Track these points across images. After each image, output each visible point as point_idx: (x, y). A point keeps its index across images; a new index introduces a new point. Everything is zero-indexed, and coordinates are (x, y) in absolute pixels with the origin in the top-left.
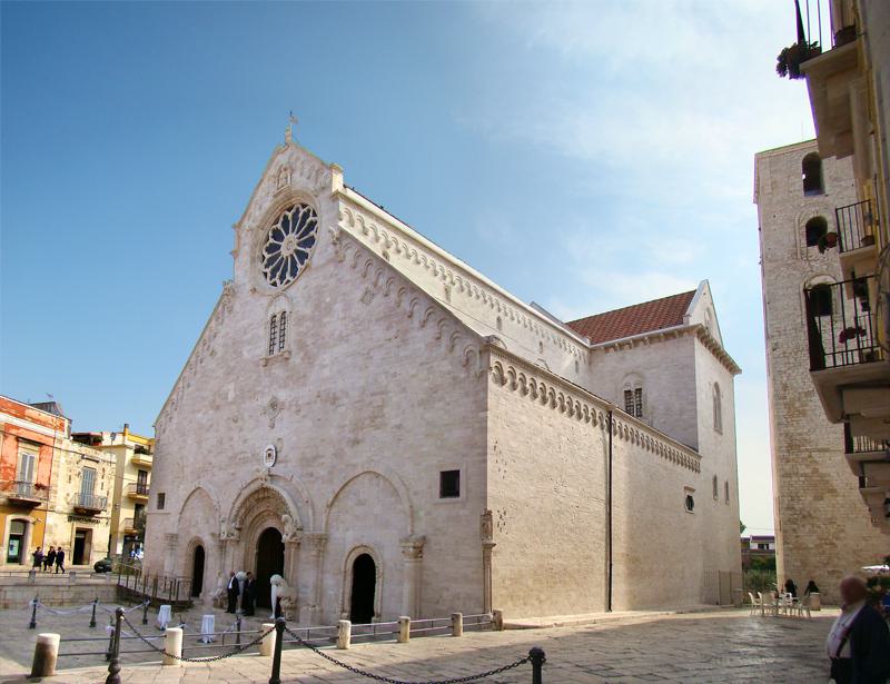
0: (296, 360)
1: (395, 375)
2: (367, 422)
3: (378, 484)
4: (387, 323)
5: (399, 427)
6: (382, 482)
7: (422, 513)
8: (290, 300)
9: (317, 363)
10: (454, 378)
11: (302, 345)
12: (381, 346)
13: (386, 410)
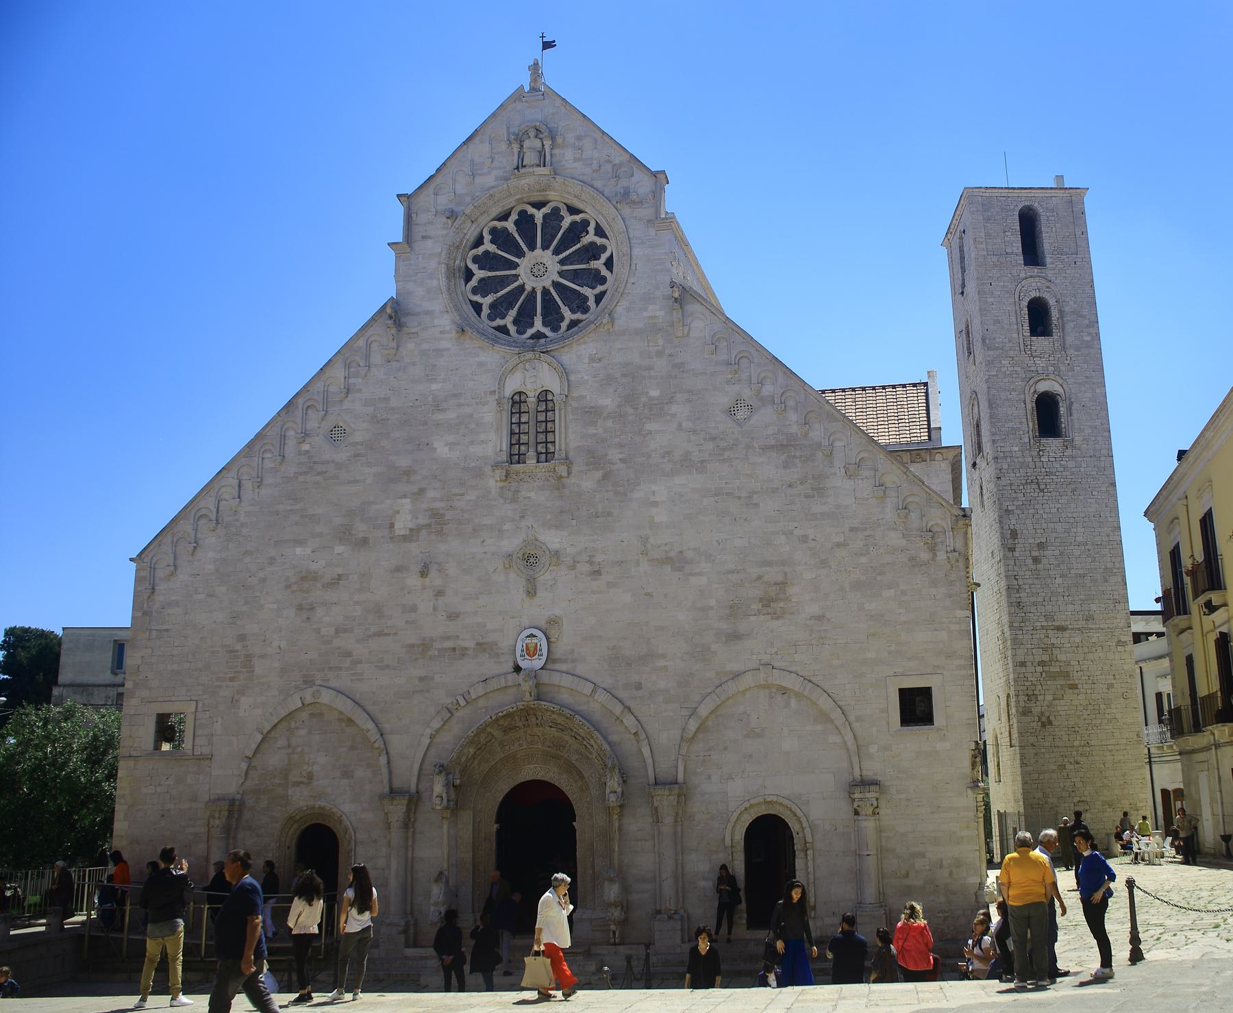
0: (586, 481)
1: (804, 539)
2: (756, 606)
3: (787, 705)
4: (784, 457)
5: (820, 618)
6: (793, 703)
7: (873, 749)
8: (565, 373)
9: (636, 495)
10: (912, 559)
11: (595, 460)
12: (774, 490)
13: (791, 590)
